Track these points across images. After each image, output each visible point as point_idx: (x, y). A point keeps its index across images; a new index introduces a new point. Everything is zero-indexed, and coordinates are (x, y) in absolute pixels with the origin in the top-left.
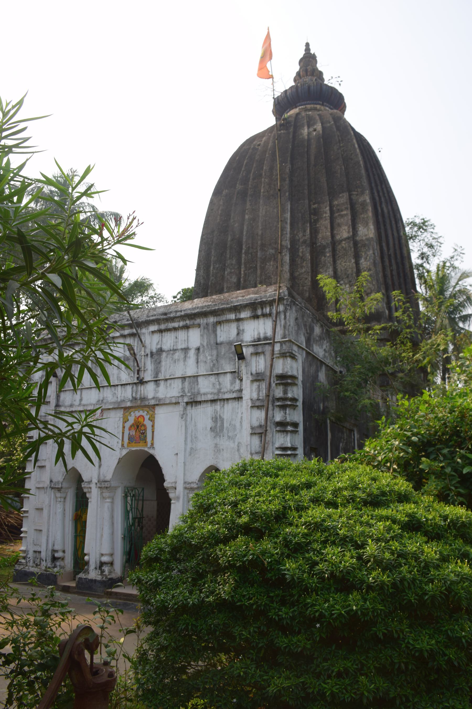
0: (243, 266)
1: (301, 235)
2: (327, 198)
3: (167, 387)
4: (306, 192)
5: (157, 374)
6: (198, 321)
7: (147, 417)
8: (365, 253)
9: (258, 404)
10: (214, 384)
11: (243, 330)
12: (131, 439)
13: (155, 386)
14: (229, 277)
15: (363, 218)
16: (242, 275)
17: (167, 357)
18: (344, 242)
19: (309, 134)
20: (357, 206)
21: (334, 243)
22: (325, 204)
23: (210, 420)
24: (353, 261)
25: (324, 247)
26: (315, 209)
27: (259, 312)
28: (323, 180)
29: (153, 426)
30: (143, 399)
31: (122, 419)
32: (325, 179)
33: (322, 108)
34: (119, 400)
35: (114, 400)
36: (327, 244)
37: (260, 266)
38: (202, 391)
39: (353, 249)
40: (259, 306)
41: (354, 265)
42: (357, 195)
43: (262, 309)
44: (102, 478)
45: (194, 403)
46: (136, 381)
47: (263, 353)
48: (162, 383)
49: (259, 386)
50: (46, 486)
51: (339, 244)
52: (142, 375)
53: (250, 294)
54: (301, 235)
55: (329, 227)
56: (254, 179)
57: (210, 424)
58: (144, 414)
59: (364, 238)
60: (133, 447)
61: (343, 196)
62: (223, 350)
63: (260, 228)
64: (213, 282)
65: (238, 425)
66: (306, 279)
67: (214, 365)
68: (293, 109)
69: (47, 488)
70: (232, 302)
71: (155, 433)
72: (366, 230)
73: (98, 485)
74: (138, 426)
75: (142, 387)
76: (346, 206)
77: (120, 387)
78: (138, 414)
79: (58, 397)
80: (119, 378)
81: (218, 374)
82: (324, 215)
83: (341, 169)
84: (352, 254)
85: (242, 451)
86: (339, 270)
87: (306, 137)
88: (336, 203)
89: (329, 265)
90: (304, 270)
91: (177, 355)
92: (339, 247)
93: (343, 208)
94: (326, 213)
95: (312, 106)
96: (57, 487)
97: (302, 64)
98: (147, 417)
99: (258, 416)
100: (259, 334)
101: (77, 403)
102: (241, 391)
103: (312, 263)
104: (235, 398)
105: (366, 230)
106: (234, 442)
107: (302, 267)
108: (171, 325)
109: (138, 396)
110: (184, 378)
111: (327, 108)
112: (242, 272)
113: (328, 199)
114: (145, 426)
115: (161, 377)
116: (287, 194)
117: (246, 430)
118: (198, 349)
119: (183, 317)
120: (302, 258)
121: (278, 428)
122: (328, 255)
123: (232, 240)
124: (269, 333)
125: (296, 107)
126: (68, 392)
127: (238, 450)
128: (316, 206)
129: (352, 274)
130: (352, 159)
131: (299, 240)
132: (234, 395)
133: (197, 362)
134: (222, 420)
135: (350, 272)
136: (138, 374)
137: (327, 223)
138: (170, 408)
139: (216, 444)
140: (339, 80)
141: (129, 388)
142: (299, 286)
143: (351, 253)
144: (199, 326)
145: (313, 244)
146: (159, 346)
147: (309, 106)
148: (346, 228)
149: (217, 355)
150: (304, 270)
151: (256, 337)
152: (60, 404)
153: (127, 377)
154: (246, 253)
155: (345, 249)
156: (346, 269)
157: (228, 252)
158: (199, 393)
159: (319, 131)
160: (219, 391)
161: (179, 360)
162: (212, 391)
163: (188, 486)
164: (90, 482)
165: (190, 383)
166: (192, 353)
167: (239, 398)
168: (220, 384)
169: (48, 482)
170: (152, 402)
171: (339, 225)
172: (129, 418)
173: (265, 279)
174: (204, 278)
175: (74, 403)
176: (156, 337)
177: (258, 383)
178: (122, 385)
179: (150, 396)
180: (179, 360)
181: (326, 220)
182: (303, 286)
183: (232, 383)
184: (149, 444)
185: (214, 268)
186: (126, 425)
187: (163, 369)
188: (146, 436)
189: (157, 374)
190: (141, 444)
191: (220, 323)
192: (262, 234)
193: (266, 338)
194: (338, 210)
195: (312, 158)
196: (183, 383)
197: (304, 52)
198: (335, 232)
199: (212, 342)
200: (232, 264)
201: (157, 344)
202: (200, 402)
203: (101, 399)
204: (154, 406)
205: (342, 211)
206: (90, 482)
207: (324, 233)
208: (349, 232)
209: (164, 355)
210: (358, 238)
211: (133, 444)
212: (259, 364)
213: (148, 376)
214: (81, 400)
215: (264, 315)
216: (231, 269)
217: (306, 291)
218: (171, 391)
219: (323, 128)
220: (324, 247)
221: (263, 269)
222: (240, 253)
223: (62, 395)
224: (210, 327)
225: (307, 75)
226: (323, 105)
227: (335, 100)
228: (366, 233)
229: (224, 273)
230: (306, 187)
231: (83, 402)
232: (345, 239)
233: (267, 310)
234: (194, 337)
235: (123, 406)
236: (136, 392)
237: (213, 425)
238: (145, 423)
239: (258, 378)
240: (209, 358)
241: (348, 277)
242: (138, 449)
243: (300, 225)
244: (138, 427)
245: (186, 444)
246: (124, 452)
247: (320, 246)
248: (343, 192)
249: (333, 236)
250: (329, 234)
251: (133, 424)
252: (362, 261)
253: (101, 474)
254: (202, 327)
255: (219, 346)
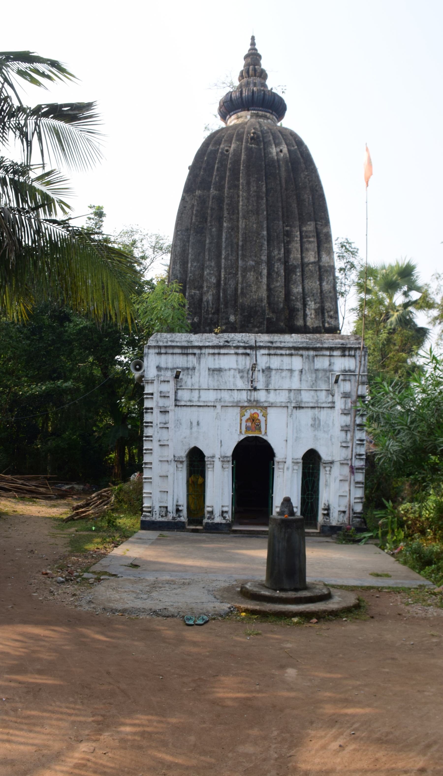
0: (223, 270)
1: (276, 252)
2: (297, 223)
3: (276, 395)
4: (280, 213)
5: (267, 385)
6: (301, 352)
7: (261, 415)
8: (327, 278)
9: (345, 412)
10: (313, 396)
11: (334, 363)
12: (247, 428)
13: (266, 393)
14: (208, 277)
15: (327, 247)
16: (223, 279)
17: (276, 374)
18: (311, 265)
19: (277, 153)
20: (321, 235)
21: (303, 265)
22: (296, 228)
23: (310, 420)
24: (318, 283)
25: (295, 267)
26: (287, 231)
27: (347, 353)
28: (295, 205)
29: (266, 421)
30: (257, 401)
31: (239, 414)
32: (296, 205)
33: (271, 116)
34: (236, 400)
35: (231, 399)
36: (298, 264)
37: (242, 274)
38: (304, 400)
39: (318, 273)
40: (348, 350)
41: (319, 287)
42: (322, 225)
43: (349, 351)
44: (223, 455)
45: (299, 407)
46: (250, 388)
47: (350, 380)
48: (272, 392)
49: (345, 401)
50: (169, 459)
51: (307, 266)
52: (255, 384)
53: (336, 339)
54: (276, 252)
55: (299, 250)
56: (229, 188)
57: (310, 422)
58: (259, 412)
59: (326, 265)
60: (249, 433)
61: (311, 224)
62: (320, 375)
63: (241, 239)
64: (191, 278)
65: (331, 424)
66: (281, 292)
67: (313, 384)
68: (244, 110)
69: (171, 461)
70: (325, 343)
71: (268, 426)
72: (328, 258)
73: (221, 459)
74: (253, 419)
75: (256, 393)
76: (313, 234)
77: (236, 391)
78: (253, 411)
79: (176, 393)
80: (234, 384)
81: (316, 390)
82: (296, 239)
83: (309, 198)
84: (318, 277)
85: (333, 440)
86: (306, 288)
87: (276, 158)
88: (304, 229)
89: (299, 283)
90: (278, 284)
91: (284, 373)
92: (307, 269)
93: (311, 235)
94: (297, 237)
95: (264, 113)
96: (181, 460)
97: (249, 60)
98: (261, 415)
99: (347, 420)
100: (345, 367)
101: (196, 399)
102: (334, 403)
103: (285, 279)
104: (329, 407)
105: (328, 258)
106: (328, 434)
107: (277, 281)
108: (279, 352)
109: (252, 399)
110: (290, 390)
111: (274, 117)
112: (223, 276)
113: (298, 224)
114: (259, 420)
115: (271, 387)
116: (265, 213)
117: (337, 428)
118: (301, 371)
119: (290, 348)
120: (277, 273)
121: (358, 428)
122: (298, 274)
123: (210, 243)
124: (352, 368)
125: (248, 110)
126: (186, 390)
127: (331, 440)
128: (288, 228)
129: (317, 294)
130: (317, 191)
131: (274, 257)
132: (330, 405)
133: (301, 381)
134: (319, 421)
135: (315, 291)
136: (252, 383)
137: (298, 245)
138: (280, 410)
139: (315, 435)
140: (284, 88)
141: (244, 393)
142: (274, 297)
143: (316, 275)
144: (302, 356)
145: (286, 262)
146: (267, 365)
147: (260, 113)
148: (313, 253)
149: (316, 378)
150: (278, 284)
151: (343, 369)
152: (178, 398)
153: (242, 384)
154: (226, 259)
155: (311, 272)
156: (312, 289)
157: (207, 253)
158: (302, 402)
159: (285, 154)
160: (317, 402)
161: (286, 377)
162: (312, 400)
163: (295, 461)
164: (213, 457)
165: (295, 394)
166: (296, 374)
167: (333, 407)
168: (317, 397)
169: (173, 457)
170: (266, 404)
171: (307, 250)
172: (245, 413)
173: (246, 287)
174: (180, 272)
175: (193, 399)
176: (266, 358)
177: (345, 399)
178: (238, 390)
179: (262, 399)
180: (286, 377)
181: (297, 243)
182: (278, 298)
183: (327, 397)
184: (263, 432)
185: (192, 266)
186: (243, 418)
187: (273, 382)
188: (260, 427)
189: (267, 385)
190: (256, 432)
191: (317, 356)
192: (243, 245)
193: (350, 371)
194: (307, 236)
195: (283, 181)
196: (289, 393)
197: (249, 47)
198: (304, 255)
199: (312, 368)
200: (211, 266)
201: (266, 363)
202: (303, 407)
203: (219, 398)
204: (266, 407)
205: (310, 237)
206: (213, 457)
207: (295, 255)
208: (315, 257)
209: (273, 372)
210: (321, 264)
211: (250, 432)
212: (346, 387)
213: (260, 385)
214: (199, 397)
215: (350, 356)
216: (210, 270)
217: (281, 302)
218: (282, 397)
219: (289, 151)
220: (295, 267)
221: (244, 277)
222: (219, 256)
223: (180, 392)
224: (311, 358)
225: (255, 76)
226: (272, 114)
227: (275, 106)
228: (329, 261)
229: (203, 273)
230: (280, 210)
231: (201, 399)
232: (312, 263)
233: (352, 353)
234: (297, 363)
235: (241, 405)
236: (251, 396)
237: (313, 423)
238: (259, 418)
239: (346, 396)
240: (310, 378)
241: (313, 295)
242: (254, 435)
243: (275, 244)
244: (253, 420)
245: (293, 434)
246: (242, 437)
247: (292, 265)
248: (311, 221)
249: (302, 258)
250: (299, 256)
251: (249, 419)
252: (324, 283)
253: (222, 453)
254: (304, 357)
255: (317, 372)
